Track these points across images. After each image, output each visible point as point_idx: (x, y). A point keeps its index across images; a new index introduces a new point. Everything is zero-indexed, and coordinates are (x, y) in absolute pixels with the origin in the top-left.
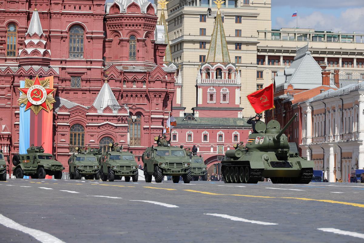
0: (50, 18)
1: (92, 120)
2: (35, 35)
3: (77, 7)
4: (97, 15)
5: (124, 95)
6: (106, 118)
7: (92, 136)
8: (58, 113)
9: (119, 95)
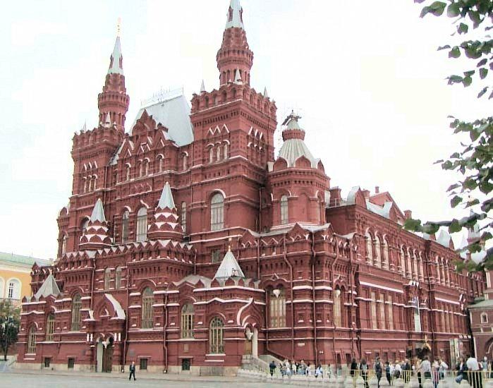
1: (201, 297)
3: (217, 174)
5: (264, 265)
6: (214, 294)
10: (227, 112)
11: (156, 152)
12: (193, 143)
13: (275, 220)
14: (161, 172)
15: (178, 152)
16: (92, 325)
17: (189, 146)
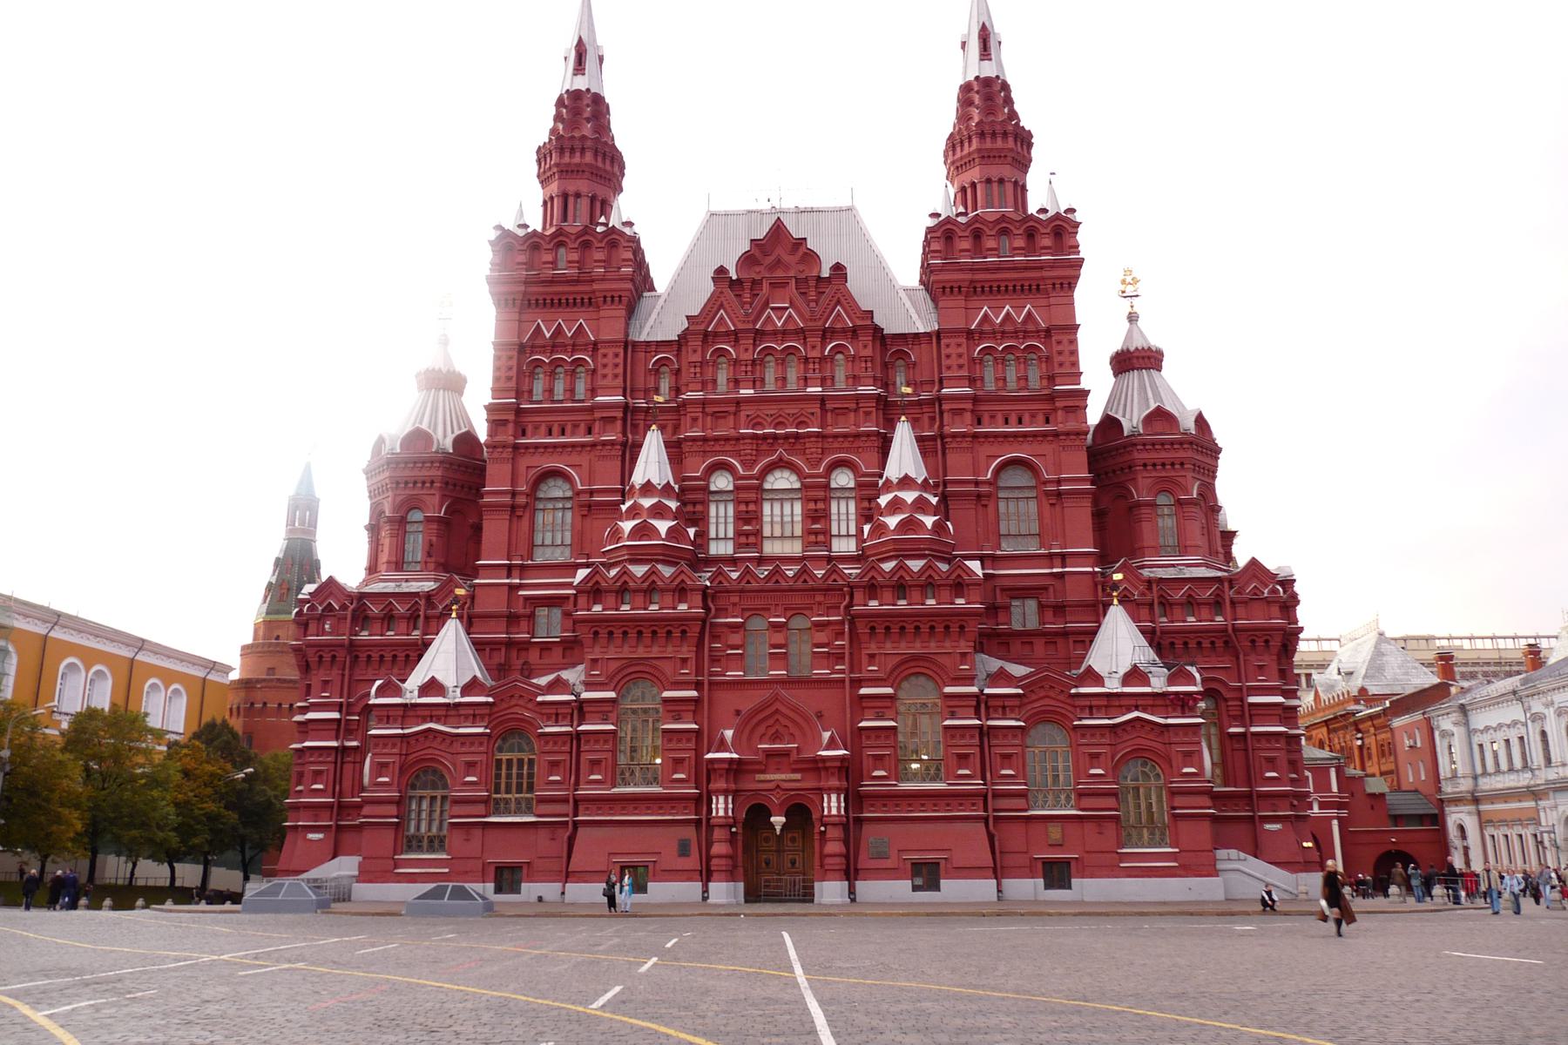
1: (1091, 707)
2: (906, 482)
3: (1013, 418)
4: (1068, 434)
7: (1097, 756)
8: (987, 691)
10: (1043, 279)
11: (827, 334)
12: (938, 334)
13: (1147, 539)
14: (841, 387)
15: (891, 349)
16: (735, 769)
17: (917, 335)
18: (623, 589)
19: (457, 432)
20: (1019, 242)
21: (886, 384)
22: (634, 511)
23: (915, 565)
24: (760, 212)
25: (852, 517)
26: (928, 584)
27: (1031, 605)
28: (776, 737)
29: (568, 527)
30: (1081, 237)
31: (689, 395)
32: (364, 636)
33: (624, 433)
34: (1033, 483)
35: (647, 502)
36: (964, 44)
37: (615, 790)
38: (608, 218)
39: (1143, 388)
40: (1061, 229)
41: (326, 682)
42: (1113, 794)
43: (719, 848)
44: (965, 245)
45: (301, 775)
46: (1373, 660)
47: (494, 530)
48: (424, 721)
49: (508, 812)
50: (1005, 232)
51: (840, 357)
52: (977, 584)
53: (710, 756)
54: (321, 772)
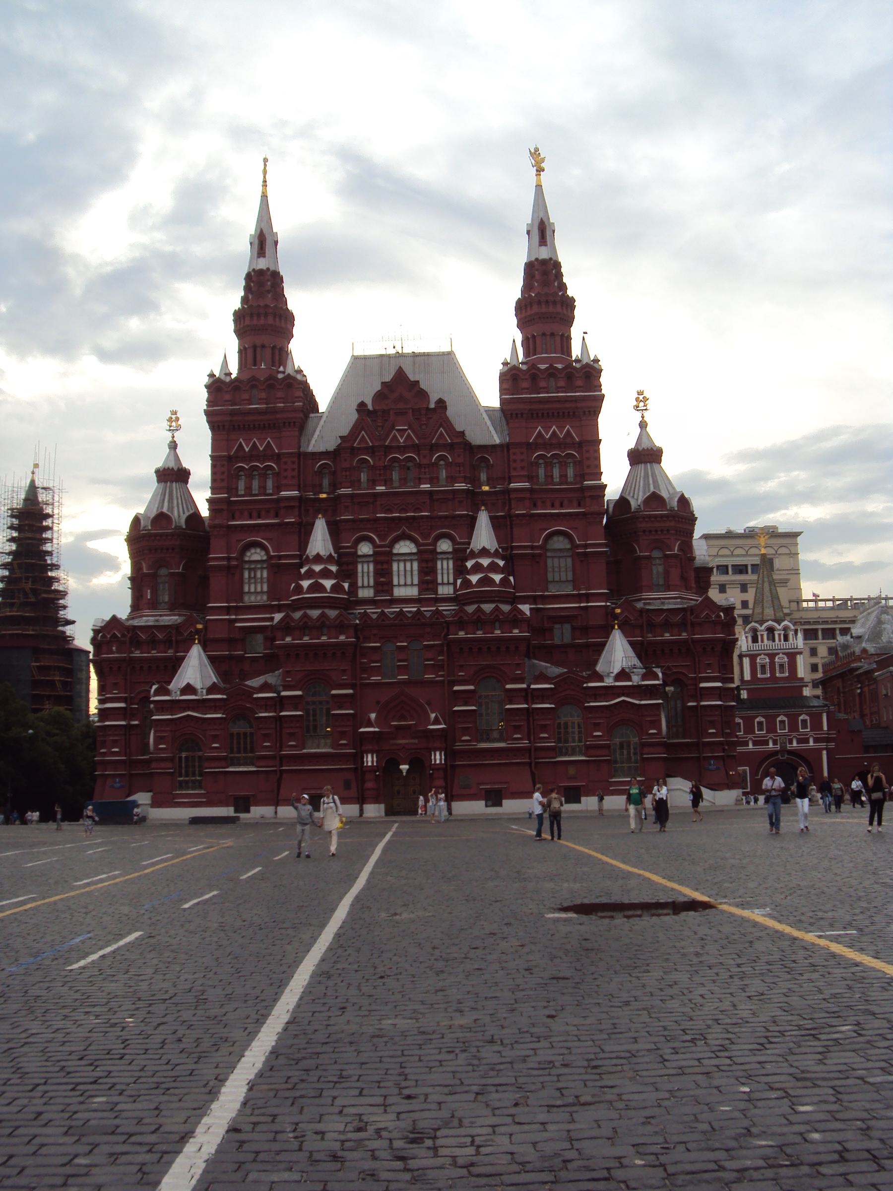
0: (511, 525)
2: (484, 552)
3: (557, 503)
4: (592, 514)
7: (598, 724)
8: (533, 686)
9: (641, 650)
10: (577, 408)
11: (433, 448)
17: (494, 447)
18: (306, 626)
19: (187, 514)
20: (562, 383)
21: (474, 481)
22: (310, 574)
23: (488, 607)
24: (389, 356)
25: (451, 571)
26: (496, 619)
27: (567, 627)
28: (402, 718)
29: (265, 580)
30: (604, 379)
31: (343, 491)
32: (137, 654)
33: (300, 516)
34: (569, 546)
35: (317, 568)
36: (528, 232)
37: (305, 751)
38: (285, 367)
39: (646, 476)
40: (590, 373)
41: (116, 684)
42: (608, 747)
43: (369, 785)
44: (525, 384)
45: (105, 741)
46: (875, 627)
47: (217, 583)
48: (184, 710)
49: (239, 765)
50: (552, 375)
51: (442, 463)
52: (527, 621)
53: (362, 730)
54: (116, 741)
